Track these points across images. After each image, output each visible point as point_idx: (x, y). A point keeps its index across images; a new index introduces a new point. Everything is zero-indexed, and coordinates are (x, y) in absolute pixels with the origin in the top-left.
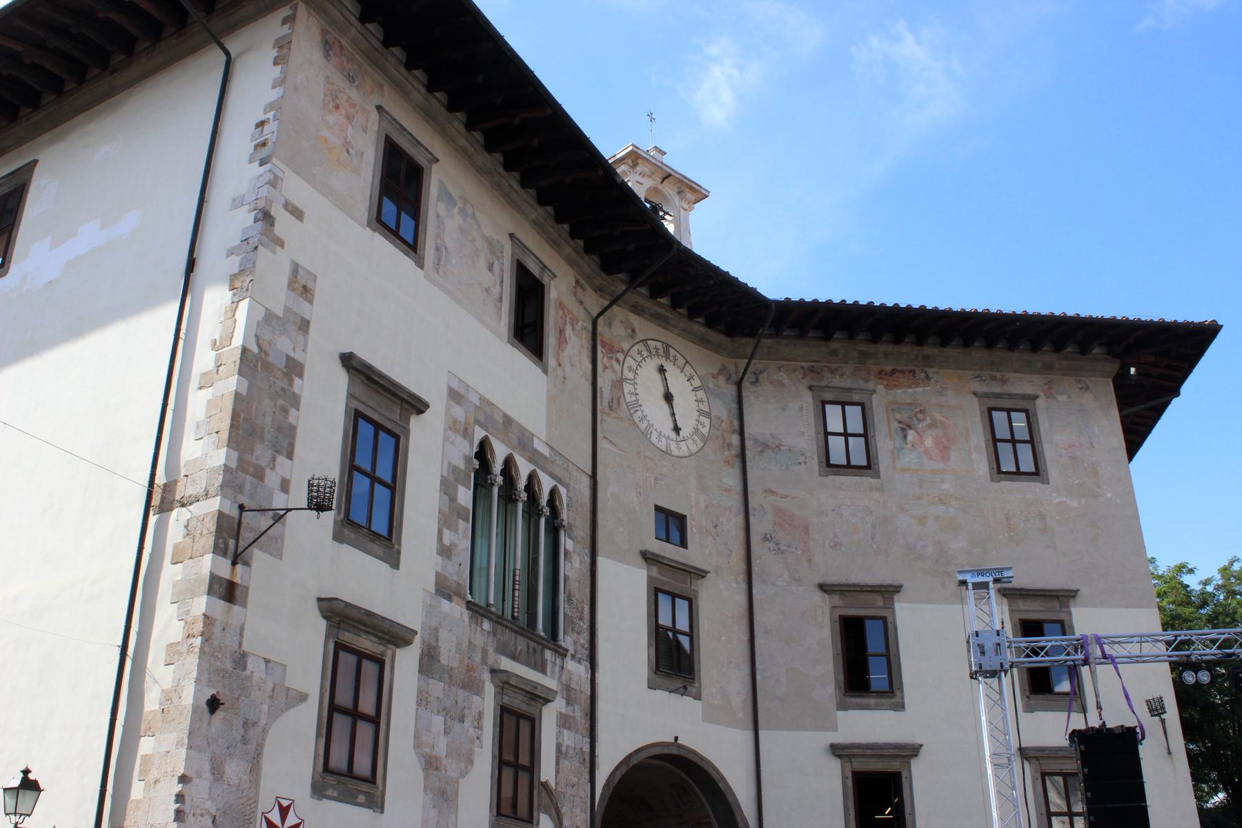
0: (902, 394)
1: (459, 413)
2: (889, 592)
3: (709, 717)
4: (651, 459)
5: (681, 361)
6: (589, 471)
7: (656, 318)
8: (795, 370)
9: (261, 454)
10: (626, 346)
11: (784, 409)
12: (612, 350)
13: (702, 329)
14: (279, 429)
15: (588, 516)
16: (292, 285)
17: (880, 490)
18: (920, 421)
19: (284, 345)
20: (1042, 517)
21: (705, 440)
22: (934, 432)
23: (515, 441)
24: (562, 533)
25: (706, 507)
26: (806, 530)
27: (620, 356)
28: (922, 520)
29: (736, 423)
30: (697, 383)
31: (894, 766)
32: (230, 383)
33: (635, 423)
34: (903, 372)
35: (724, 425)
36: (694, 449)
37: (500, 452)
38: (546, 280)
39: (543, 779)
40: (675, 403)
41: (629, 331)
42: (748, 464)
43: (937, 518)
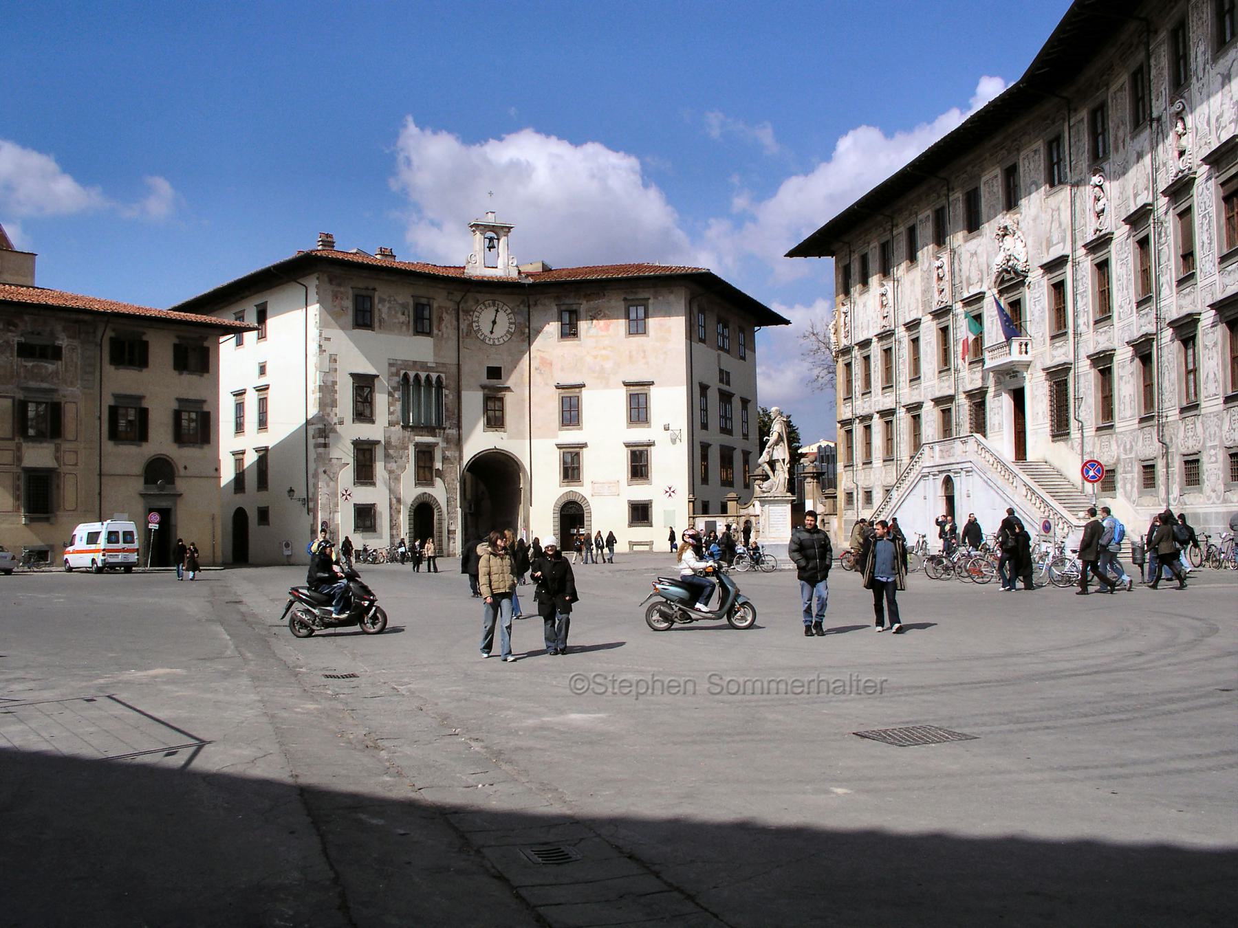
3: (510, 438)
9: (328, 409)
12: (467, 312)
19: (330, 379)
21: (512, 334)
28: (595, 357)
32: (318, 395)
37: (412, 374)
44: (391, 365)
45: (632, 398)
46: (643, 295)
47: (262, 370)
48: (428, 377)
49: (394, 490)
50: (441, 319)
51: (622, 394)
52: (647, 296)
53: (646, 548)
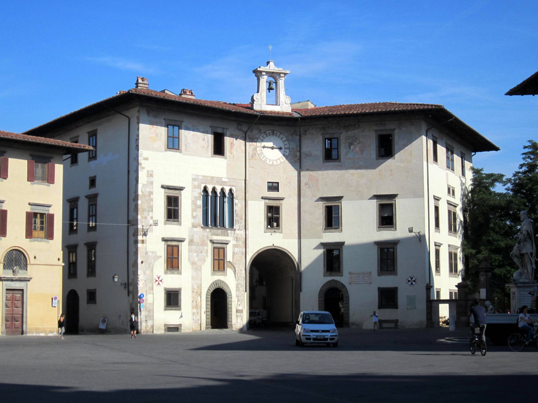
1: (196, 183)
10: (257, 136)
14: (149, 207)
16: (147, 176)
18: (355, 142)
19: (148, 190)
20: (391, 170)
22: (358, 145)
26: (318, 181)
30: (285, 139)
31: (338, 247)
38: (225, 132)
39: (228, 260)
42: (302, 161)
43: (357, 174)
44: (194, 180)
45: (382, 207)
46: (390, 126)
47: (93, 182)
48: (222, 190)
49: (195, 280)
51: (374, 204)
52: (392, 127)
53: (392, 325)
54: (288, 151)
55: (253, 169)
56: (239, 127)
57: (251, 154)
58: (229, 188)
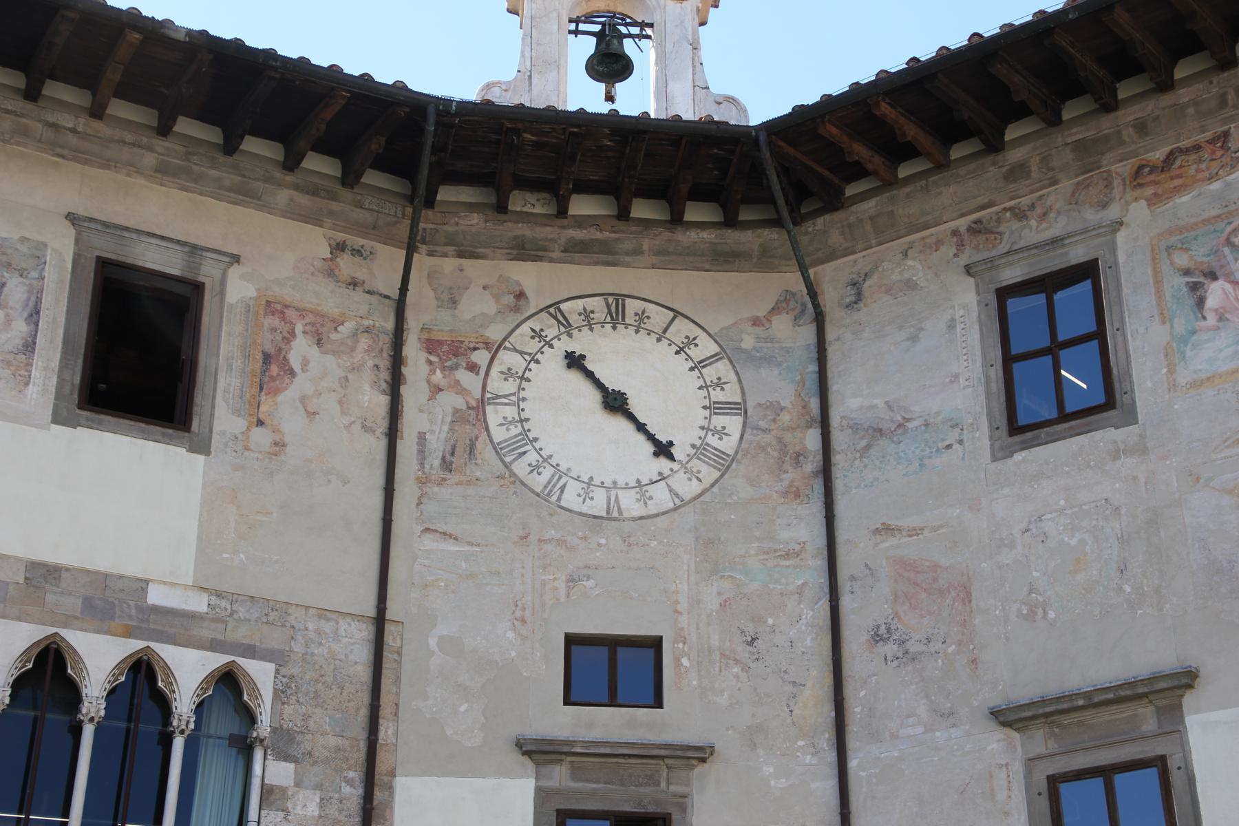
0: (1189, 205)
2: (1170, 690)
4: (561, 542)
5: (659, 317)
6: (372, 612)
7: (578, 251)
8: (939, 243)
10: (495, 333)
11: (914, 339)
12: (450, 351)
13: (707, 235)
15: (365, 698)
17: (1141, 450)
23: (72, 605)
24: (258, 755)
25: (723, 605)
26: (967, 598)
27: (481, 357)
29: (814, 404)
30: (706, 347)
33: (516, 480)
34: (1197, 148)
35: (786, 418)
36: (686, 488)
38: (208, 272)
40: (635, 406)
41: (510, 299)
42: (839, 484)
50: (271, 368)
54: (733, 424)
55: (451, 547)
56: (347, 265)
57: (437, 446)
58: (217, 661)
